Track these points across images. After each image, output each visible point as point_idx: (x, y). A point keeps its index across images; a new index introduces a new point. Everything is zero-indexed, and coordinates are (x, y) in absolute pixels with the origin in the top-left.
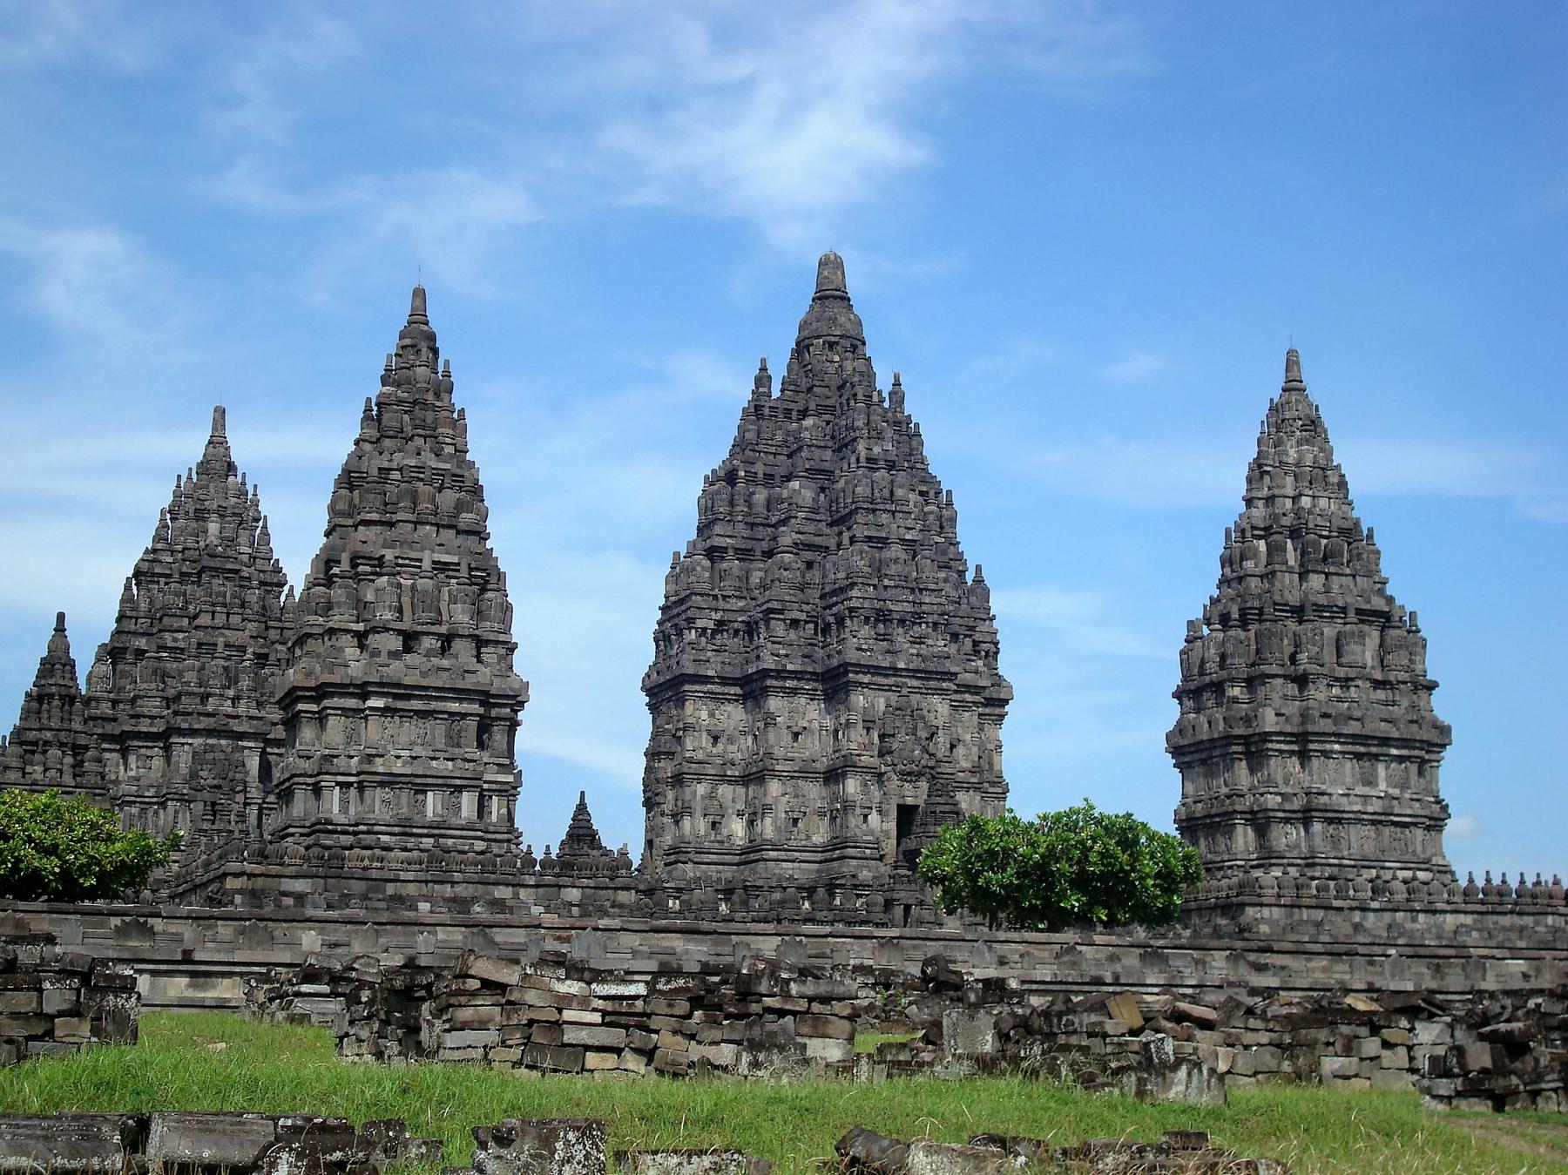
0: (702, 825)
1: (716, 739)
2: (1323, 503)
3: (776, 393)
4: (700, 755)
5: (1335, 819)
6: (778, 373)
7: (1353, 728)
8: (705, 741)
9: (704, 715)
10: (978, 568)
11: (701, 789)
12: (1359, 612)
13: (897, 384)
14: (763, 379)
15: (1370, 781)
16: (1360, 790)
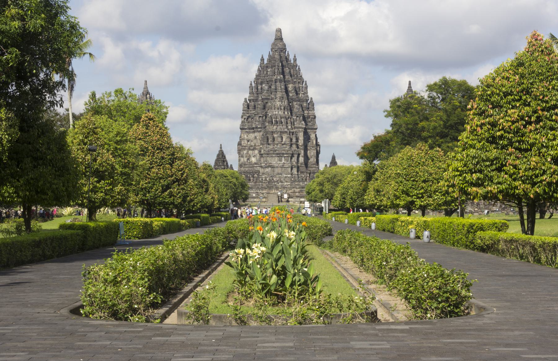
0: (245, 159)
1: (248, 141)
2: (280, 112)
3: (266, 62)
4: (245, 145)
5: (273, 167)
6: (266, 58)
7: (277, 152)
8: (246, 142)
9: (246, 136)
10: (311, 98)
11: (245, 152)
12: (281, 132)
13: (295, 57)
14: (262, 60)
15: (281, 161)
16: (279, 162)
